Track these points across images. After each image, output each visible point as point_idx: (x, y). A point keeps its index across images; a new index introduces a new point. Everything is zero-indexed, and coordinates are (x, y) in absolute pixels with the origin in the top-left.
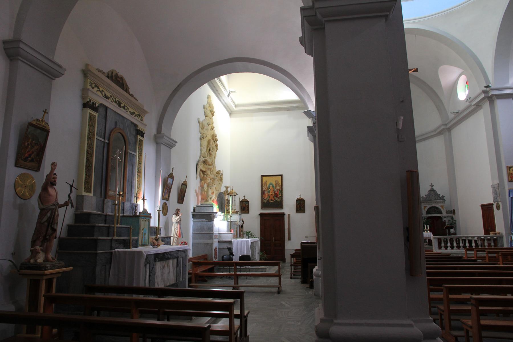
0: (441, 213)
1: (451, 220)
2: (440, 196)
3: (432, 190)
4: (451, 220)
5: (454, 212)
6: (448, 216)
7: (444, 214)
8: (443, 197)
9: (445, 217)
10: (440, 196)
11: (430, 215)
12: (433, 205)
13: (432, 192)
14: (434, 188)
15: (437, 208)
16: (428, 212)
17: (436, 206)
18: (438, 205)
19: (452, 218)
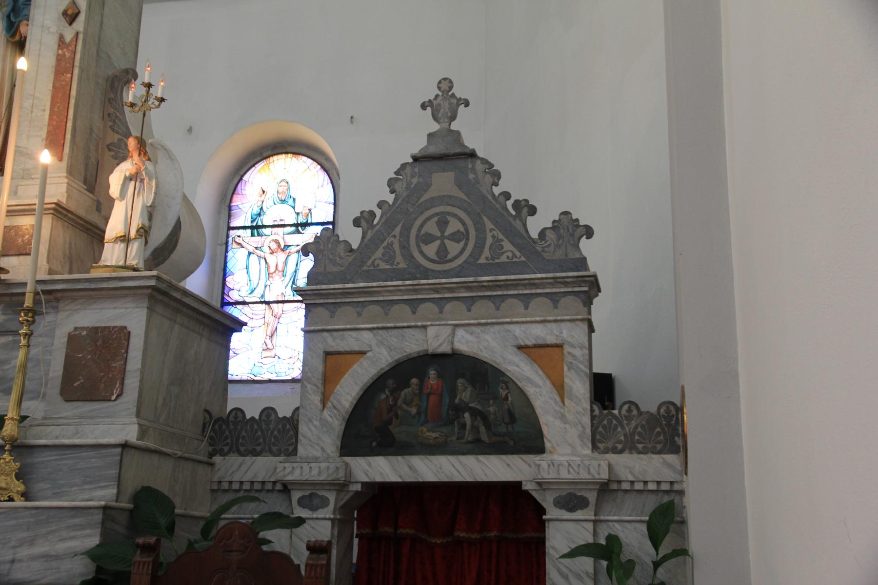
0: (533, 443)
1: (634, 539)
2: (535, 226)
3: (448, 156)
4: (634, 539)
5: (666, 429)
6: (606, 489)
7: (567, 451)
8: (571, 229)
9: (572, 502)
10: (535, 226)
11: (383, 469)
12: (436, 339)
13: (443, 182)
14: (472, 130)
15: (481, 374)
16: (367, 429)
17: (466, 342)
18: (489, 341)
19: (667, 520)
